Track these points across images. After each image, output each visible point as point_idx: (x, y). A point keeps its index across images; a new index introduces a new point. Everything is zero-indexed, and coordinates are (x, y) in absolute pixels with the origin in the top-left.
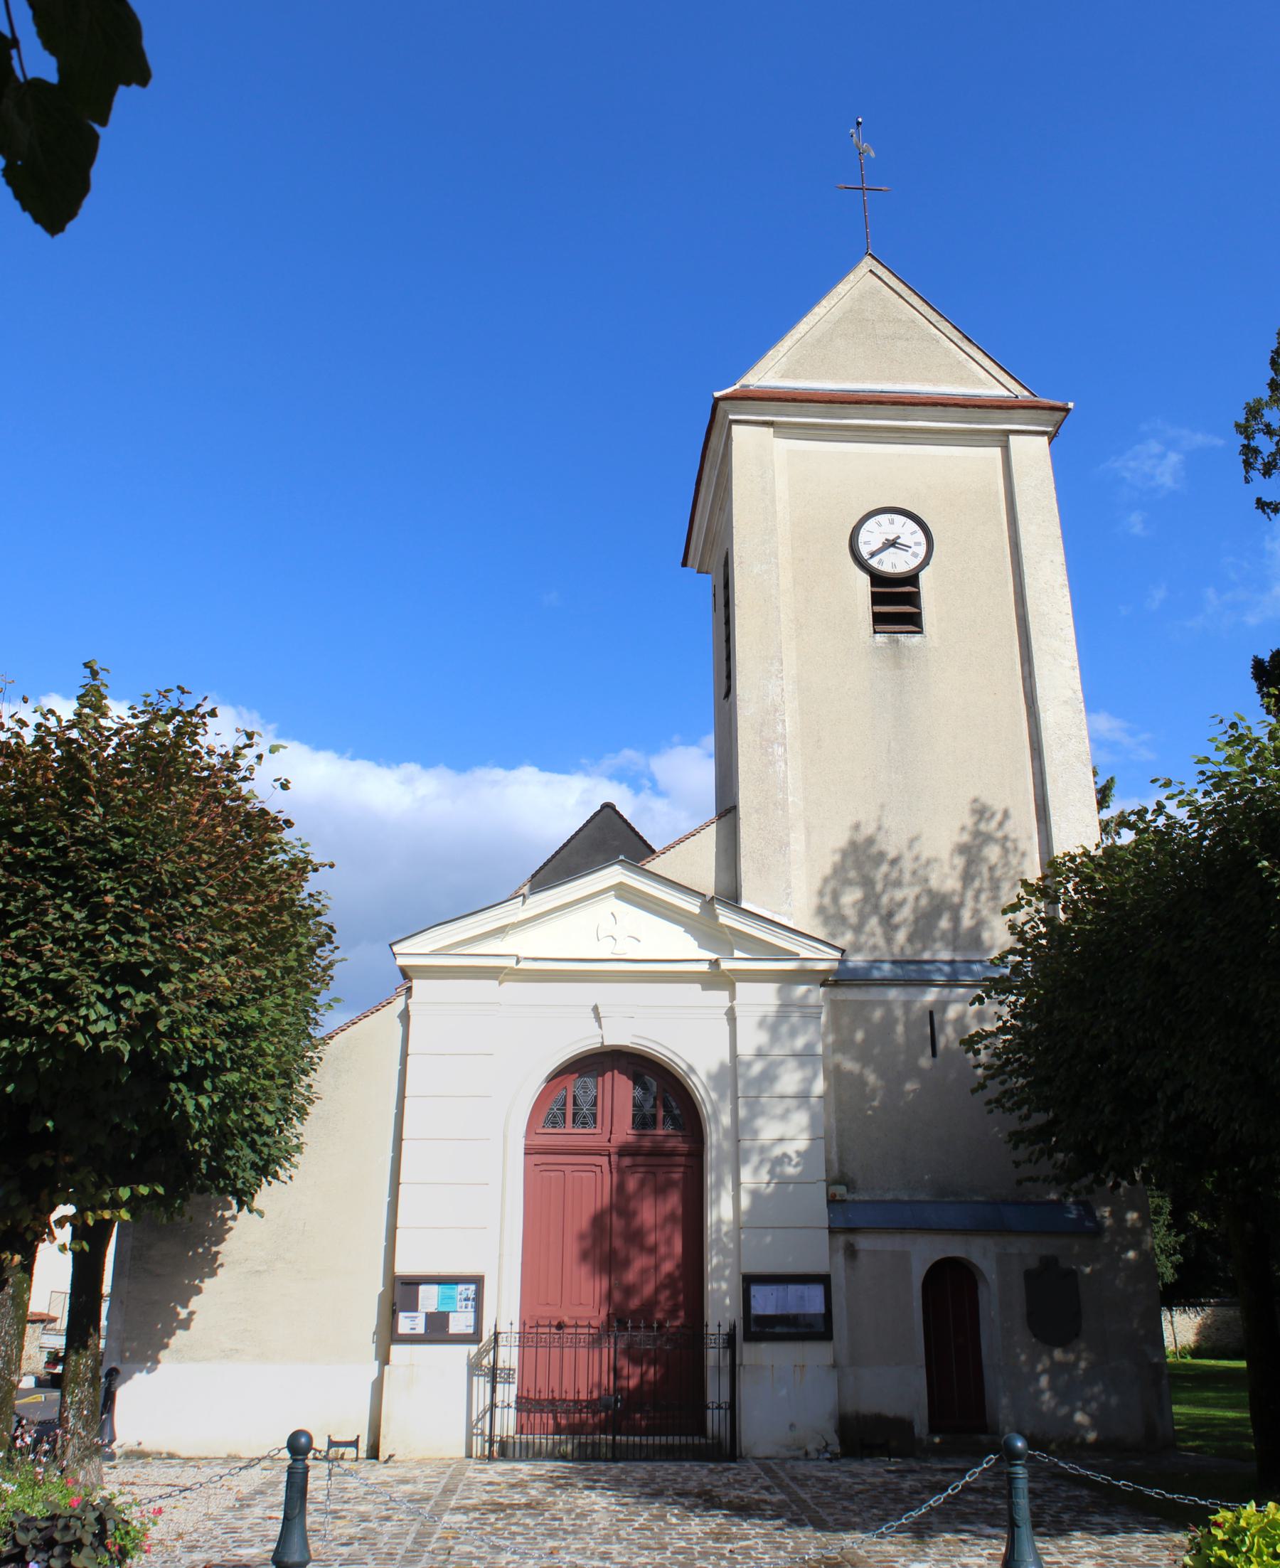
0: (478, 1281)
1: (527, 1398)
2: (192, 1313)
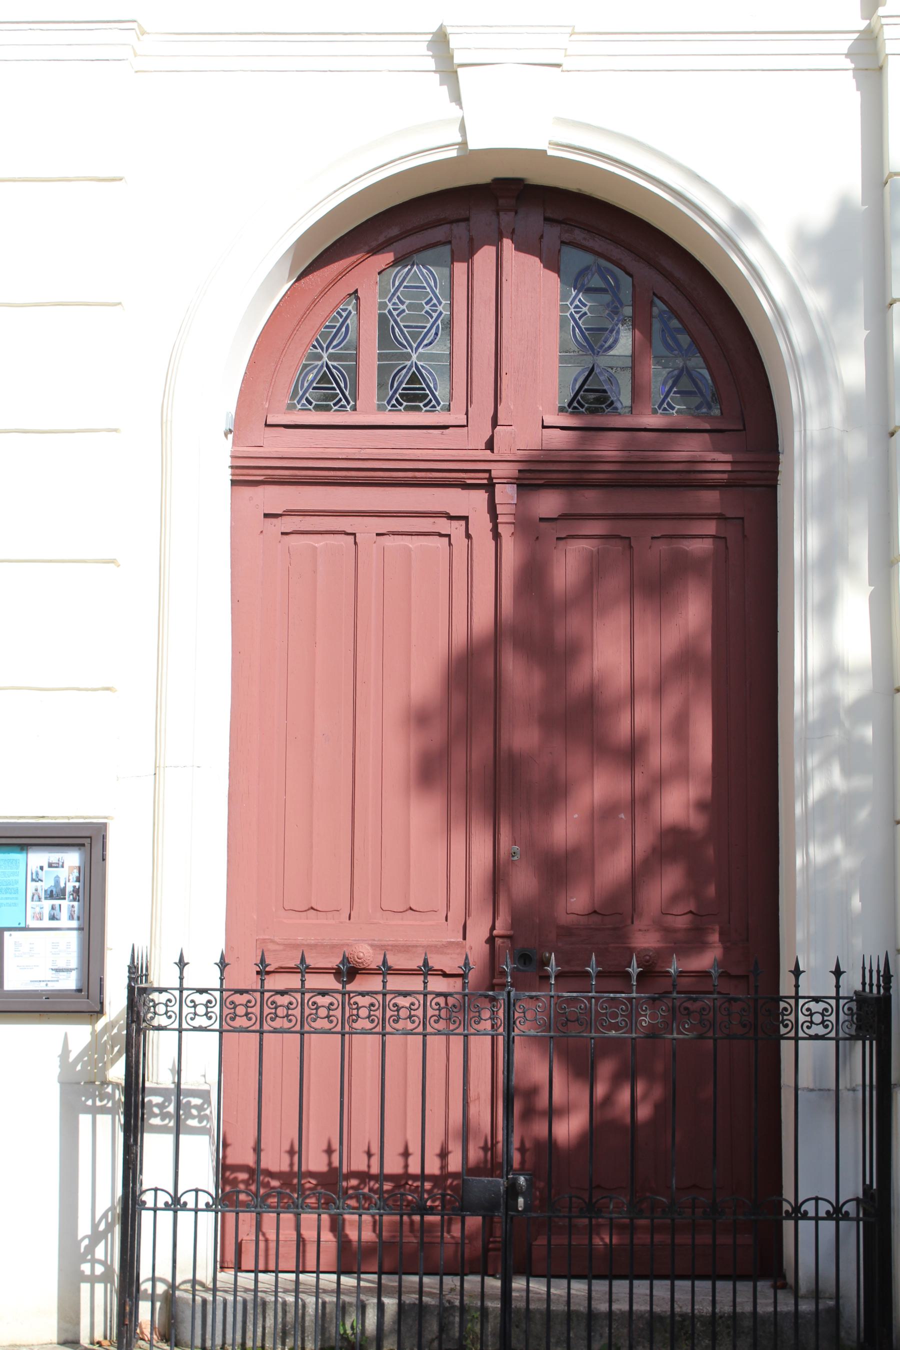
1: (255, 1172)
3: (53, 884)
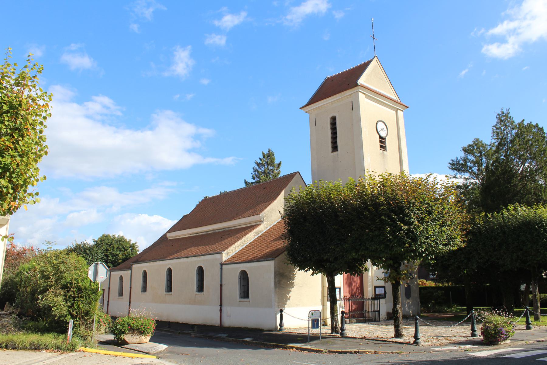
2: (290, 296)
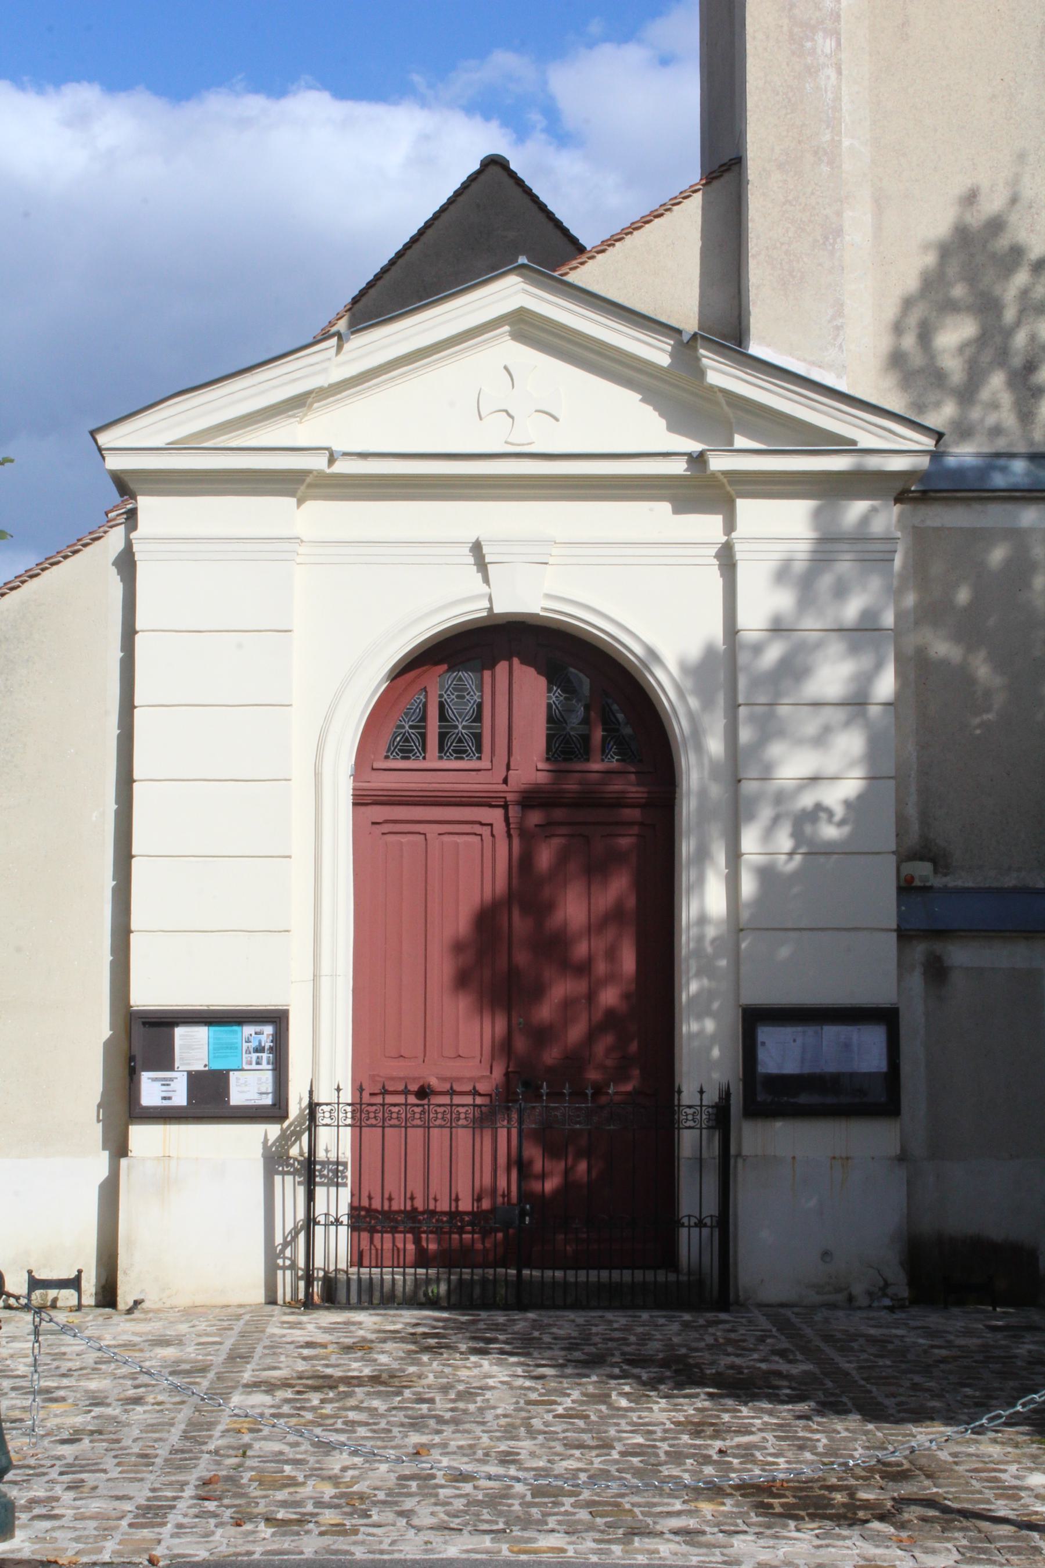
0: (278, 1019)
1: (369, 1210)
3: (257, 1044)
